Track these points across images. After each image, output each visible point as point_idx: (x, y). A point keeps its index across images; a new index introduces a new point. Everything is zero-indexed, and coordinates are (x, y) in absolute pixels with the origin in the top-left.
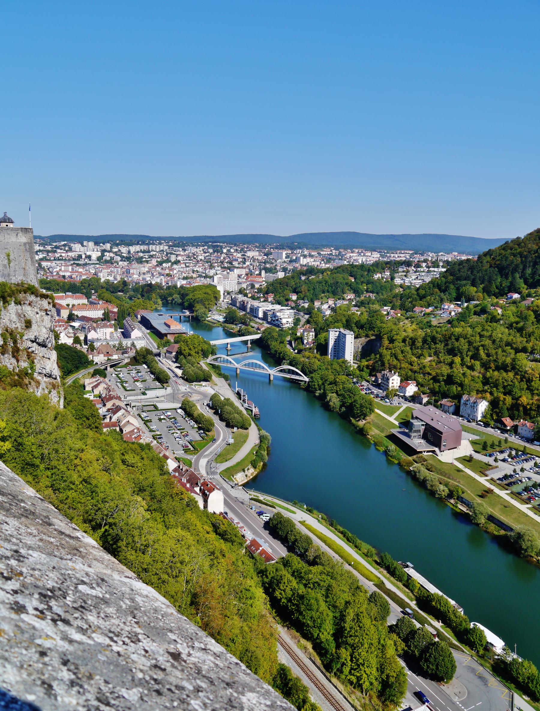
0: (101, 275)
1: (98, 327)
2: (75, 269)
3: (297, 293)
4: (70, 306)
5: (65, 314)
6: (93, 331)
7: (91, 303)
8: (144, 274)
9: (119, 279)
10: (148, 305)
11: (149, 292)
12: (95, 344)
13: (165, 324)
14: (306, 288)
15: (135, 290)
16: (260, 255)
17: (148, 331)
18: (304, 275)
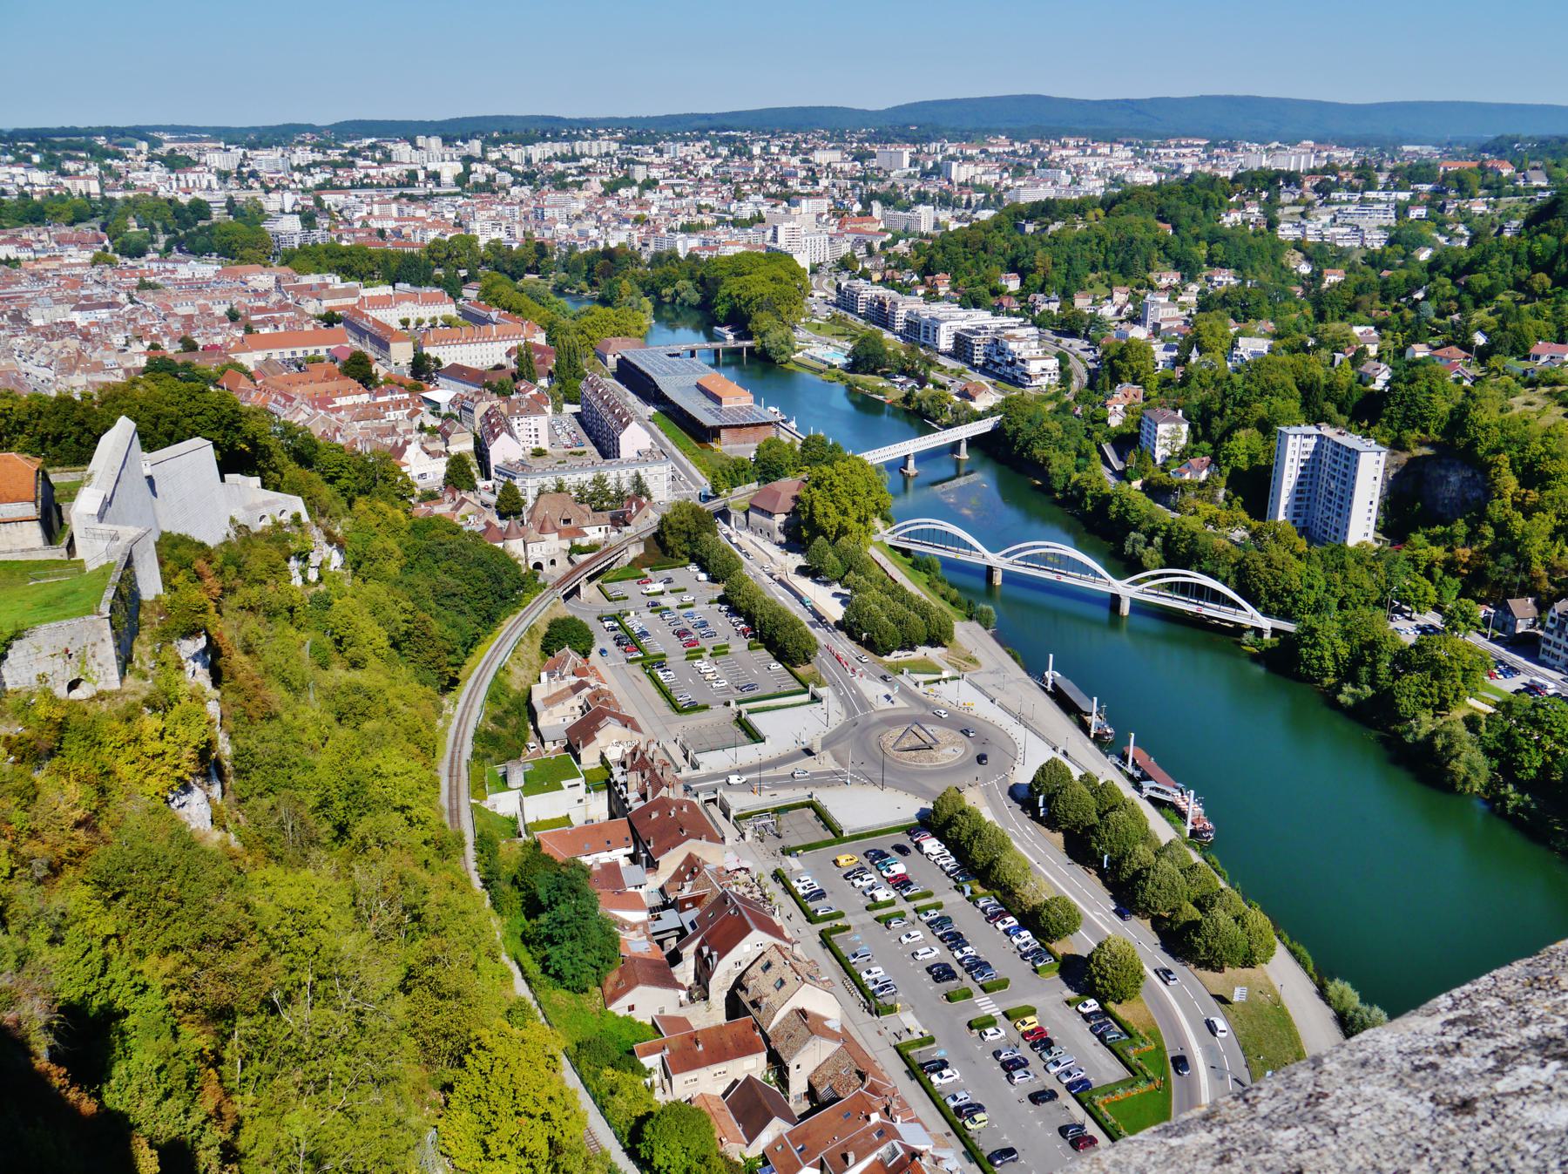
0: (476, 227)
1: (512, 413)
2: (406, 210)
3: (1023, 274)
4: (412, 325)
5: (402, 354)
6: (504, 436)
7: (466, 314)
8: (578, 218)
9: (518, 231)
10: (631, 324)
11: (607, 273)
12: (517, 482)
13: (699, 387)
14: (1048, 258)
15: (569, 266)
16: (844, 160)
17: (652, 410)
18: (1030, 219)
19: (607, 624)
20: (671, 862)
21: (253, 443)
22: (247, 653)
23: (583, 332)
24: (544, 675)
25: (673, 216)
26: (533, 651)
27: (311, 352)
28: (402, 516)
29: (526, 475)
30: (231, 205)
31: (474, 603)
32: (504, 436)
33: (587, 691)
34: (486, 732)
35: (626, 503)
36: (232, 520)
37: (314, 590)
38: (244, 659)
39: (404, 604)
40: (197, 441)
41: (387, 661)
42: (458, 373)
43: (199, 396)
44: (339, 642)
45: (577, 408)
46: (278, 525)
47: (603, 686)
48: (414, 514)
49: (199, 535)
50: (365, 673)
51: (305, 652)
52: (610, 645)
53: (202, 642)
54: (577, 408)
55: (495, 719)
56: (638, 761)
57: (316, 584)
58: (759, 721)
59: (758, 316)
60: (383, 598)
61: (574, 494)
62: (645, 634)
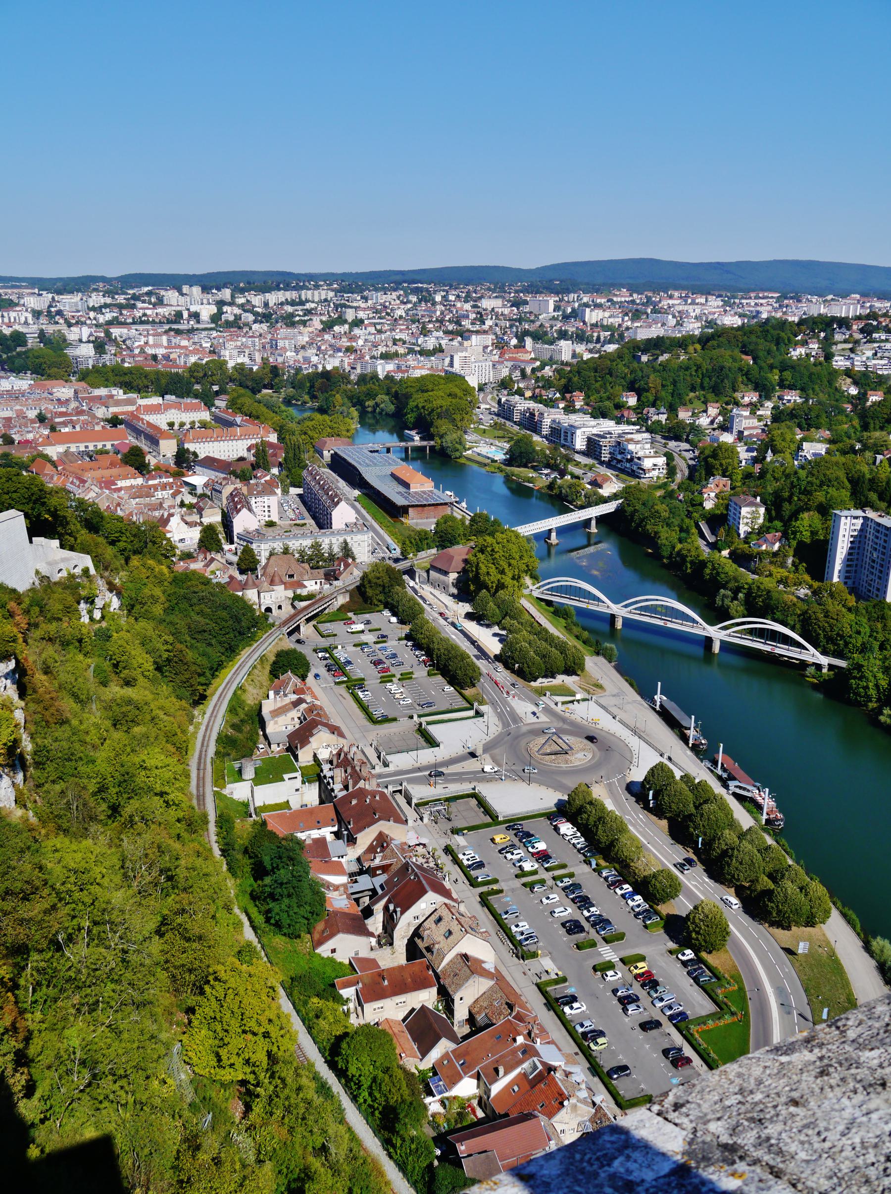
0: (226, 354)
1: (251, 493)
2: (174, 341)
3: (639, 393)
4: (176, 427)
5: (168, 448)
6: (244, 511)
7: (217, 419)
8: (303, 347)
9: (258, 357)
11: (324, 389)
12: (254, 546)
13: (393, 475)
14: (659, 381)
16: (504, 306)
17: (357, 493)
18: (644, 352)
19: (320, 655)
20: (366, 838)
21: (54, 514)
22: (46, 673)
23: (305, 433)
24: (271, 693)
25: (375, 346)
26: (263, 675)
27: (100, 446)
28: (165, 570)
29: (260, 541)
30: (42, 335)
31: (220, 638)
32: (244, 511)
33: (304, 706)
34: (226, 736)
35: (336, 563)
36: (37, 572)
37: (97, 626)
38: (44, 677)
39: (166, 637)
40: (12, 512)
41: (152, 681)
42: (210, 463)
43: (14, 478)
44: (116, 666)
45: (300, 491)
46: (72, 576)
47: (317, 702)
48: (175, 569)
49: (11, 584)
50: (135, 689)
51: (90, 673)
52: (322, 671)
53: (12, 665)
54: (300, 491)
55: (233, 726)
56: (342, 760)
57: (100, 622)
58: (435, 731)
59: (439, 422)
60: (151, 632)
61: (297, 555)
62: (349, 663)
